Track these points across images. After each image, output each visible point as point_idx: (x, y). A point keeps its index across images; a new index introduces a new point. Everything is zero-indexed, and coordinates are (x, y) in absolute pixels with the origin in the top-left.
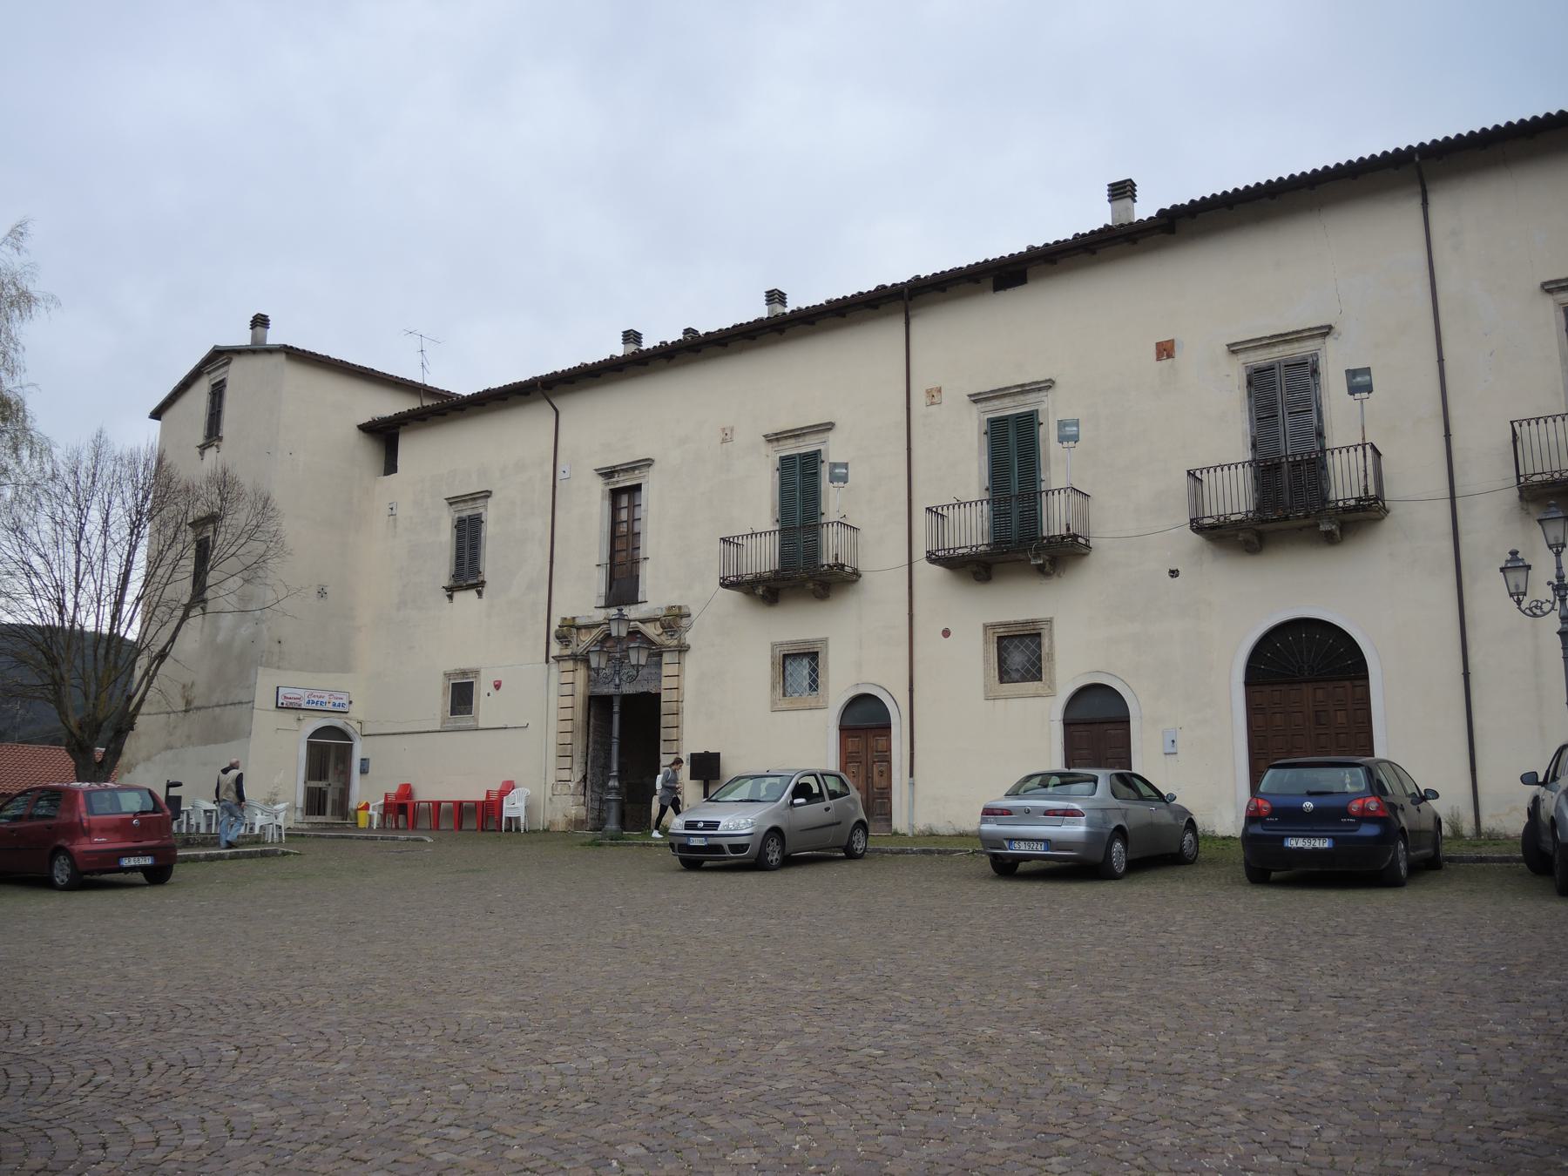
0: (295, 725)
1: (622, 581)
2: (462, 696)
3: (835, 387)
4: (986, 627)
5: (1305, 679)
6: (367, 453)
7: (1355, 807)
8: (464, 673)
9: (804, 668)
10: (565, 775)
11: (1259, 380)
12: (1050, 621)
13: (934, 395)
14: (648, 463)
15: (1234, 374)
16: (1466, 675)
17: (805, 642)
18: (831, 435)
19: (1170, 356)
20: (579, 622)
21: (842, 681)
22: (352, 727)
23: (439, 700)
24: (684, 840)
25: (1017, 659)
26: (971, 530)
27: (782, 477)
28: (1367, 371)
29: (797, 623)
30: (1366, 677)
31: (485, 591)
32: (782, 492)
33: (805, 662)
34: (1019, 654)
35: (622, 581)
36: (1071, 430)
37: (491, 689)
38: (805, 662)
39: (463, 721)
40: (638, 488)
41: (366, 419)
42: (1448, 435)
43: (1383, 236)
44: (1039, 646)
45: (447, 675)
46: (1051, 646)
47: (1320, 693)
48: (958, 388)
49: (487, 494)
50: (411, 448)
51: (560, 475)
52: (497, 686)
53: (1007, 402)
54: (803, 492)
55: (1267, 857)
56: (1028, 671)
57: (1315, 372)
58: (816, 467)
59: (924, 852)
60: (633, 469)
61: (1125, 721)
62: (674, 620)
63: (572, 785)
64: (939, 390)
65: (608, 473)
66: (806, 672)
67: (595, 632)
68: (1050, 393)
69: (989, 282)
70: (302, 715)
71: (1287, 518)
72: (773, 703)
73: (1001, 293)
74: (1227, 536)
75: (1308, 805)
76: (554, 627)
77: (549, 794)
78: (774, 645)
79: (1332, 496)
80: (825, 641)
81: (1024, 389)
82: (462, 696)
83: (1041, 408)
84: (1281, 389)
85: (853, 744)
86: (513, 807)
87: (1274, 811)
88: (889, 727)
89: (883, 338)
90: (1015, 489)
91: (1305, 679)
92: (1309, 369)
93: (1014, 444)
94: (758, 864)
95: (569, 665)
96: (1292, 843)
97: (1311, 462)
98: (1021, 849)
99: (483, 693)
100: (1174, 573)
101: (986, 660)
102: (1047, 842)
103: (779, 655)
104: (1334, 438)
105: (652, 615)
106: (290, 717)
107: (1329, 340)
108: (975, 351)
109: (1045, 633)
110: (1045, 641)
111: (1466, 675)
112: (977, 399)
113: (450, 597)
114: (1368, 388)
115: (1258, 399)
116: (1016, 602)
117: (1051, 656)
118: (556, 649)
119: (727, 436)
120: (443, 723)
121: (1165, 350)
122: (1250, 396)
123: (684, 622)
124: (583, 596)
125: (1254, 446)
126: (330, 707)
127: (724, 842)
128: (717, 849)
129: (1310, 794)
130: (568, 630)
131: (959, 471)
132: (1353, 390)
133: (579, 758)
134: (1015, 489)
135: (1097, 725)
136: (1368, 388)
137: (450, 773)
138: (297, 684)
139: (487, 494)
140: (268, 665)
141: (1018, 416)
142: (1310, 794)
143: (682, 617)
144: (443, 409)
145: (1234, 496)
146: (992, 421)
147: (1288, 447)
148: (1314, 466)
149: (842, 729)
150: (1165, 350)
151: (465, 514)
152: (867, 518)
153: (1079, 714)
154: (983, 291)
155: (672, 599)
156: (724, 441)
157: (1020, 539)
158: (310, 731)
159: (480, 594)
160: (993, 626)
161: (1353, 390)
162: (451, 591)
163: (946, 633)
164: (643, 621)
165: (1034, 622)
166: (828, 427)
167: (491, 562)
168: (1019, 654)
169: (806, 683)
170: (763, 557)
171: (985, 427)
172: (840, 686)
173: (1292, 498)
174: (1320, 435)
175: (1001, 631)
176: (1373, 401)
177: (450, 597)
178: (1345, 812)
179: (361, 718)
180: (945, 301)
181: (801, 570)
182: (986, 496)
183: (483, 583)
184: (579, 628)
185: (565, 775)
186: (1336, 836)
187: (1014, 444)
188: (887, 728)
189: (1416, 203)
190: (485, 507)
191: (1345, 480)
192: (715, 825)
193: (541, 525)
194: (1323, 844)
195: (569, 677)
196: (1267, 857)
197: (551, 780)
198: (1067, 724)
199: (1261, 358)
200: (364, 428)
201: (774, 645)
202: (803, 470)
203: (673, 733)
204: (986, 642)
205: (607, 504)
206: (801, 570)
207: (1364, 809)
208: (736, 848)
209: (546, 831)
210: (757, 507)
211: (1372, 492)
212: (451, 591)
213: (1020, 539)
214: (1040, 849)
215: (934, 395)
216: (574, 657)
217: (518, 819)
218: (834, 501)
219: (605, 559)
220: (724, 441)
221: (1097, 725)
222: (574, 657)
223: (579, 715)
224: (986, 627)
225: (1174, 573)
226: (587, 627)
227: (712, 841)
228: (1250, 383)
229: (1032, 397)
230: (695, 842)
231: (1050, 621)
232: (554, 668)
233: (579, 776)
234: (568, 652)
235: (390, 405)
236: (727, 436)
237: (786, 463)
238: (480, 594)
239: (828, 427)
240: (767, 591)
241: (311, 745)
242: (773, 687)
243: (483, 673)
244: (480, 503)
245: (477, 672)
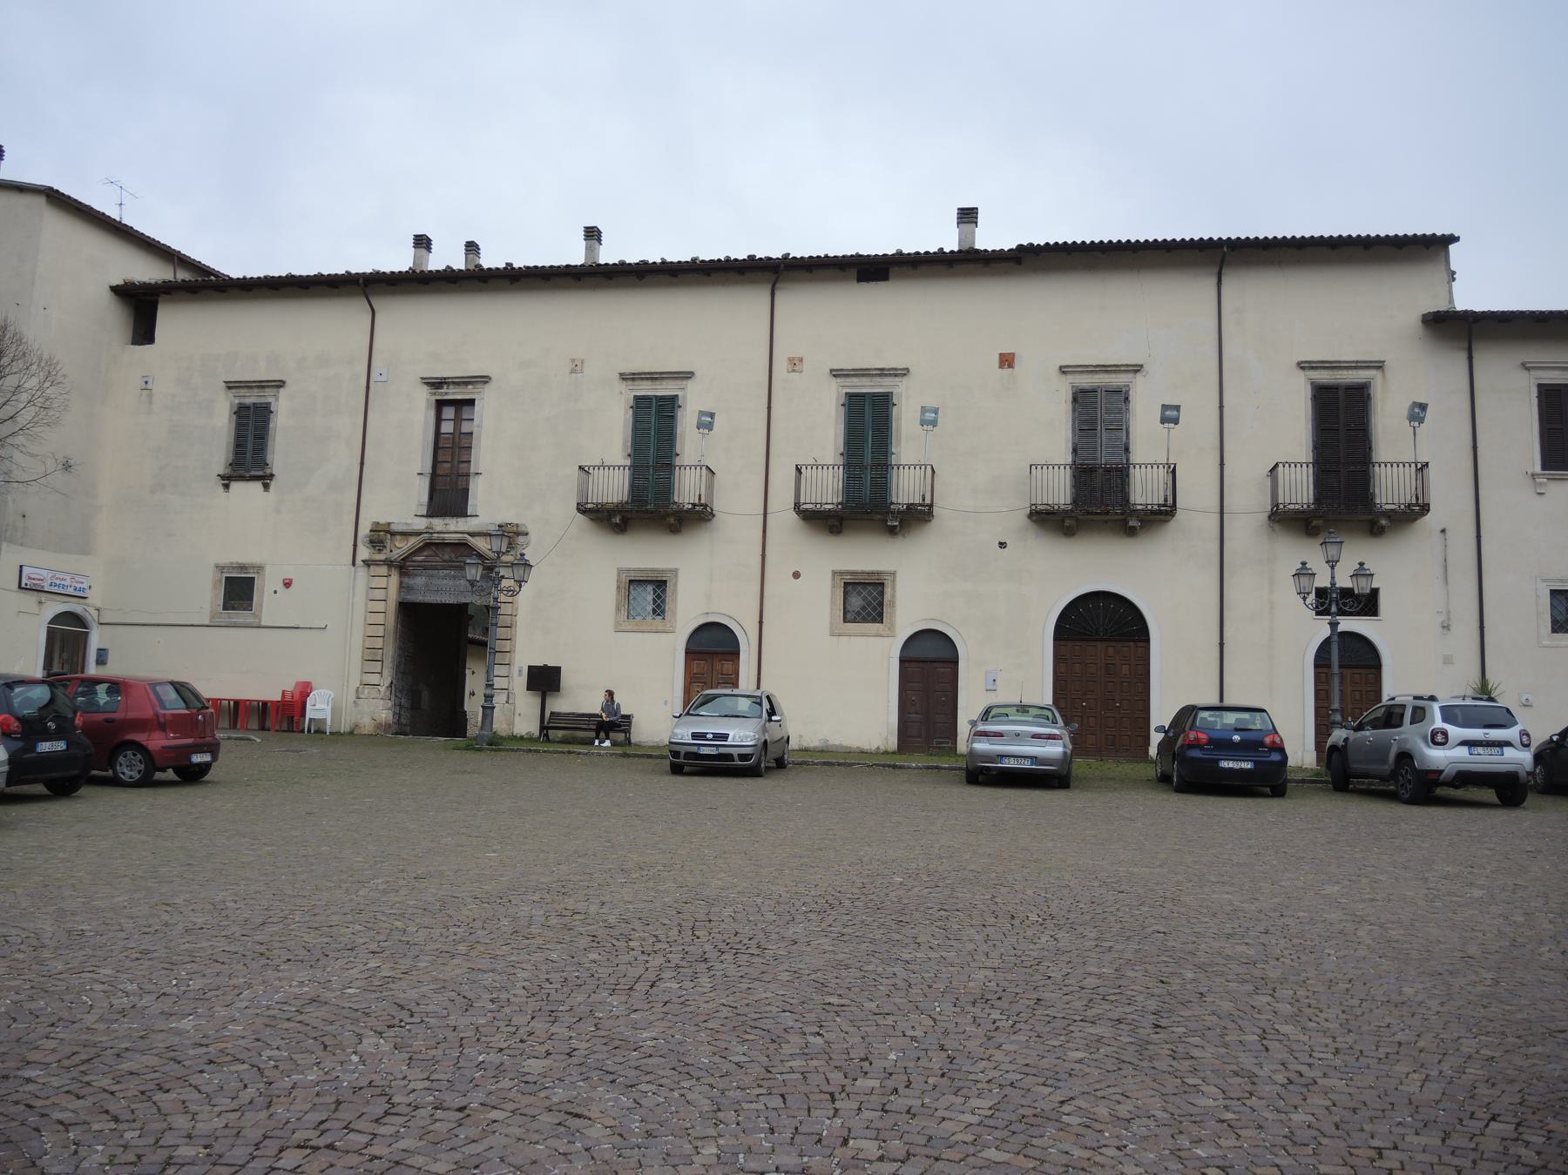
0: (35, 609)
1: (448, 488)
2: (239, 591)
3: (708, 346)
4: (834, 573)
5: (1101, 634)
6: (116, 319)
7: (1268, 740)
8: (243, 568)
9: (648, 594)
10: (375, 679)
11: (1082, 398)
12: (894, 574)
13: (795, 364)
14: (485, 380)
15: (1062, 392)
16: (1222, 645)
17: (653, 570)
18: (690, 384)
19: (1011, 366)
20: (394, 528)
21: (690, 608)
22: (91, 615)
23: (208, 596)
24: (694, 749)
25: (856, 602)
26: (827, 490)
27: (635, 415)
28: (1177, 408)
29: (646, 553)
30: (1148, 641)
31: (273, 485)
32: (635, 429)
33: (650, 588)
34: (865, 600)
35: (448, 488)
36: (931, 416)
37: (280, 587)
38: (650, 588)
39: (239, 616)
40: (471, 402)
41: (118, 281)
42: (1222, 464)
43: (1183, 301)
44: (882, 594)
45: (220, 568)
46: (893, 596)
47: (1111, 650)
48: (820, 362)
49: (280, 384)
50: (171, 321)
51: (374, 376)
52: (287, 584)
53: (865, 381)
54: (658, 431)
55: (1341, 773)
56: (869, 614)
57: (1127, 399)
58: (673, 410)
59: (825, 764)
60: (467, 384)
61: (953, 662)
62: (510, 534)
63: (382, 689)
64: (801, 360)
65: (436, 384)
66: (650, 598)
67: (413, 541)
68: (904, 379)
69: (854, 272)
70: (43, 597)
71: (1108, 513)
72: (617, 623)
73: (864, 284)
74: (1051, 521)
75: (1236, 738)
76: (365, 530)
77: (352, 697)
78: (620, 571)
79: (1132, 500)
80: (675, 572)
81: (882, 373)
82: (239, 591)
83: (895, 391)
84: (1097, 408)
85: (698, 666)
86: (318, 707)
87: (1211, 741)
88: (737, 654)
89: (749, 304)
90: (868, 459)
91: (1101, 634)
92: (1122, 396)
93: (868, 419)
94: (753, 772)
95: (383, 570)
96: (1225, 764)
97: (1117, 470)
98: (1010, 764)
99: (268, 590)
100: (1002, 545)
101: (833, 602)
102: (1034, 759)
103: (625, 579)
104: (1137, 456)
105: (484, 529)
106: (30, 600)
107: (1139, 376)
108: (840, 334)
109: (888, 584)
110: (888, 591)
111: (1222, 645)
112: (837, 374)
113: (227, 487)
114: (1176, 421)
115: (1081, 414)
116: (864, 554)
117: (893, 603)
118: (364, 553)
119: (576, 367)
120: (213, 616)
121: (1007, 361)
122: (1074, 410)
123: (521, 539)
124: (401, 500)
125: (1075, 451)
126: (70, 591)
127: (735, 751)
128: (729, 757)
129: (1237, 730)
130: (380, 536)
131: (816, 439)
132: (1164, 420)
133: (388, 662)
134: (868, 459)
135: (929, 668)
136: (1176, 421)
137: (233, 669)
138: (43, 565)
139: (280, 384)
140: (11, 541)
141: (874, 395)
142: (1237, 730)
143: (518, 534)
144: (205, 286)
145: (1059, 492)
146: (850, 396)
147: (1104, 458)
148: (1120, 474)
149: (688, 652)
150: (1007, 361)
151: (248, 401)
152: (710, 458)
153: (915, 653)
154: (846, 279)
155: (508, 516)
156: (573, 371)
157: (868, 499)
158: (50, 615)
159: (266, 487)
160: (841, 573)
161: (1164, 420)
162: (227, 480)
163: (796, 575)
164: (472, 535)
165: (878, 573)
166: (688, 375)
167: (279, 455)
168: (865, 600)
169: (650, 608)
170: (614, 487)
171: (842, 400)
172: (688, 612)
173: (1100, 499)
174: (1127, 450)
175: (848, 578)
176: (1176, 430)
177: (227, 487)
178: (1262, 744)
179: (99, 605)
180: (811, 280)
181: (651, 501)
182: (840, 461)
183: (272, 475)
184: (393, 534)
185: (375, 679)
186: (1371, 760)
187: (868, 419)
188: (735, 654)
189: (1214, 280)
190: (276, 397)
191: (1144, 490)
192: (725, 737)
193: (349, 425)
194: (1248, 765)
195: (382, 582)
196: (1341, 773)
197: (355, 683)
198: (903, 661)
199: (1086, 381)
200: (116, 290)
201: (620, 571)
202: (658, 412)
203: (507, 646)
204: (833, 586)
205: (432, 413)
206: (651, 501)
207: (1197, 739)
208: (743, 757)
209: (351, 733)
210: (608, 442)
211: (1170, 501)
212: (227, 480)
213: (868, 499)
214: (1027, 765)
215: (795, 364)
216: (389, 563)
217: (324, 720)
218: (690, 444)
219: (428, 469)
220: (573, 371)
221: (929, 668)
222: (389, 563)
223: (391, 619)
224: (834, 573)
225: (1002, 545)
226: (405, 534)
227: (722, 750)
228: (1075, 400)
229: (888, 381)
230: (705, 751)
231: (894, 574)
232: (362, 572)
233: (387, 683)
234: (382, 557)
235: (147, 271)
236: (576, 367)
237: (640, 404)
238: (266, 487)
239: (688, 375)
240: (612, 519)
241: (51, 634)
242: (618, 609)
243: (268, 569)
244: (268, 392)
245: (260, 568)
